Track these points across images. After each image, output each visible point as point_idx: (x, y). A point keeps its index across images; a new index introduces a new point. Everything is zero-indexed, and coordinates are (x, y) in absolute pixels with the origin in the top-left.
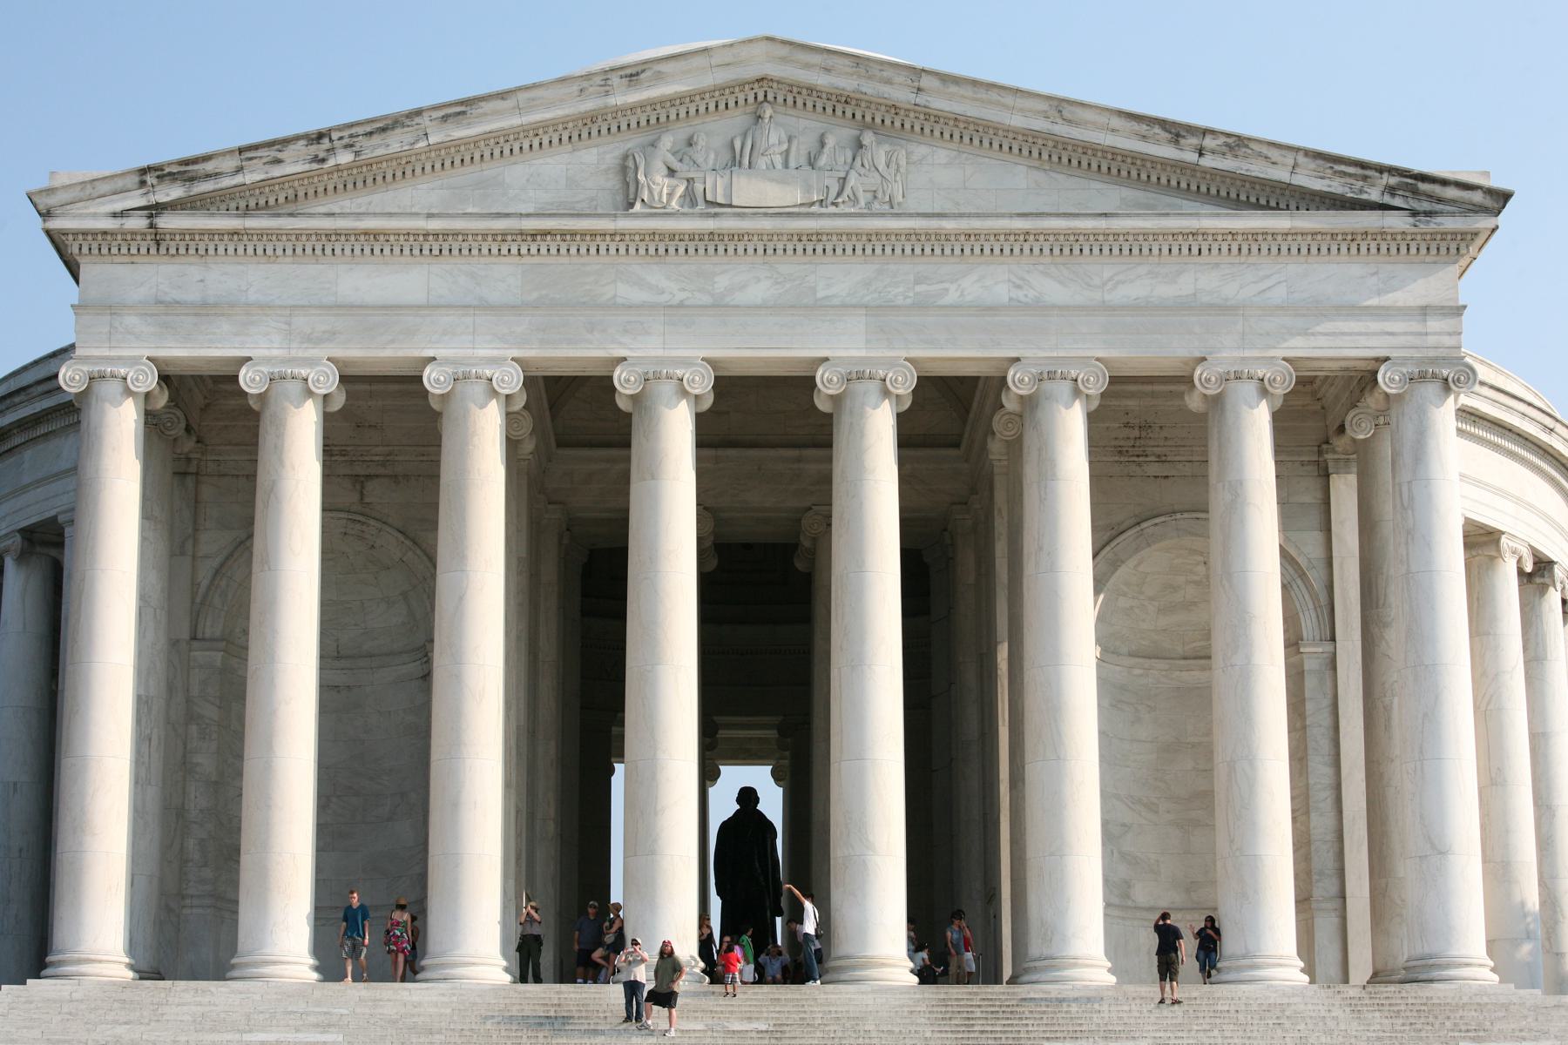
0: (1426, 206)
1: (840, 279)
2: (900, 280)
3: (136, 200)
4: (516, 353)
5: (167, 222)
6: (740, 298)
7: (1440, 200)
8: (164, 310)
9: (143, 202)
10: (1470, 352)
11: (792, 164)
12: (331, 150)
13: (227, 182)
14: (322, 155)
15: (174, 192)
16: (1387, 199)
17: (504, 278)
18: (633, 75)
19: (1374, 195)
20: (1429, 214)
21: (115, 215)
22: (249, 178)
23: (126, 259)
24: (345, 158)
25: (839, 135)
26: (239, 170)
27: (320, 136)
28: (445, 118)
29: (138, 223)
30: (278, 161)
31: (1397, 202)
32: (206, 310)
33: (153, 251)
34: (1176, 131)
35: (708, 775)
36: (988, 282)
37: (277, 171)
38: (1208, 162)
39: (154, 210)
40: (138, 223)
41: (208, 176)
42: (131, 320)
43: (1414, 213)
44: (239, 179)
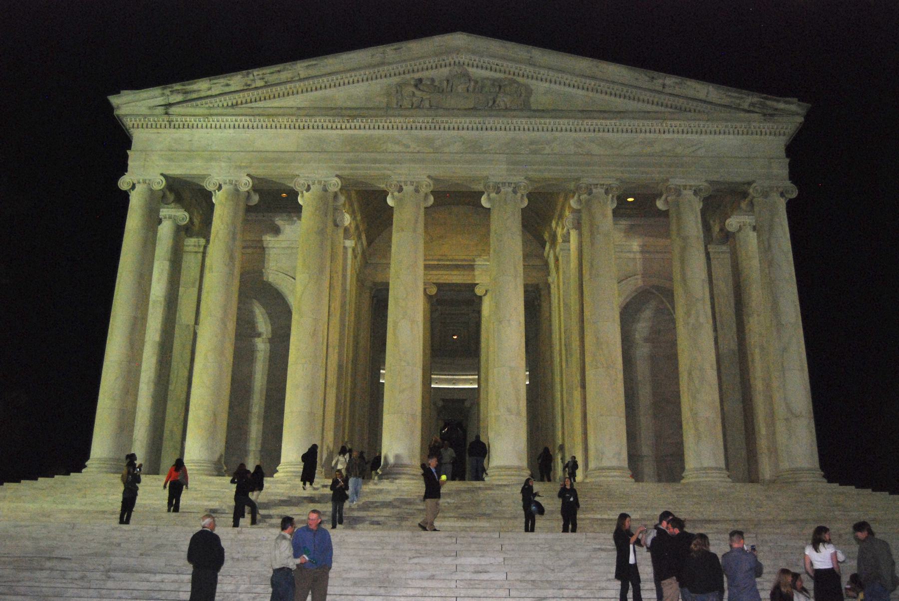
0: (770, 111)
3: (161, 101)
4: (338, 173)
5: (172, 110)
6: (447, 150)
7: (776, 109)
8: (172, 153)
9: (163, 103)
11: (471, 89)
12: (254, 80)
13: (203, 94)
14: (249, 83)
15: (180, 98)
16: (752, 108)
19: (746, 106)
20: (771, 115)
21: (150, 108)
22: (214, 92)
23: (155, 130)
24: (260, 83)
26: (210, 89)
28: (308, 67)
30: (228, 85)
31: (757, 110)
32: (191, 154)
33: (168, 126)
35: (427, 381)
37: (227, 89)
38: (667, 90)
39: (170, 105)
40: (161, 110)
41: (194, 91)
43: (765, 115)
44: (209, 93)
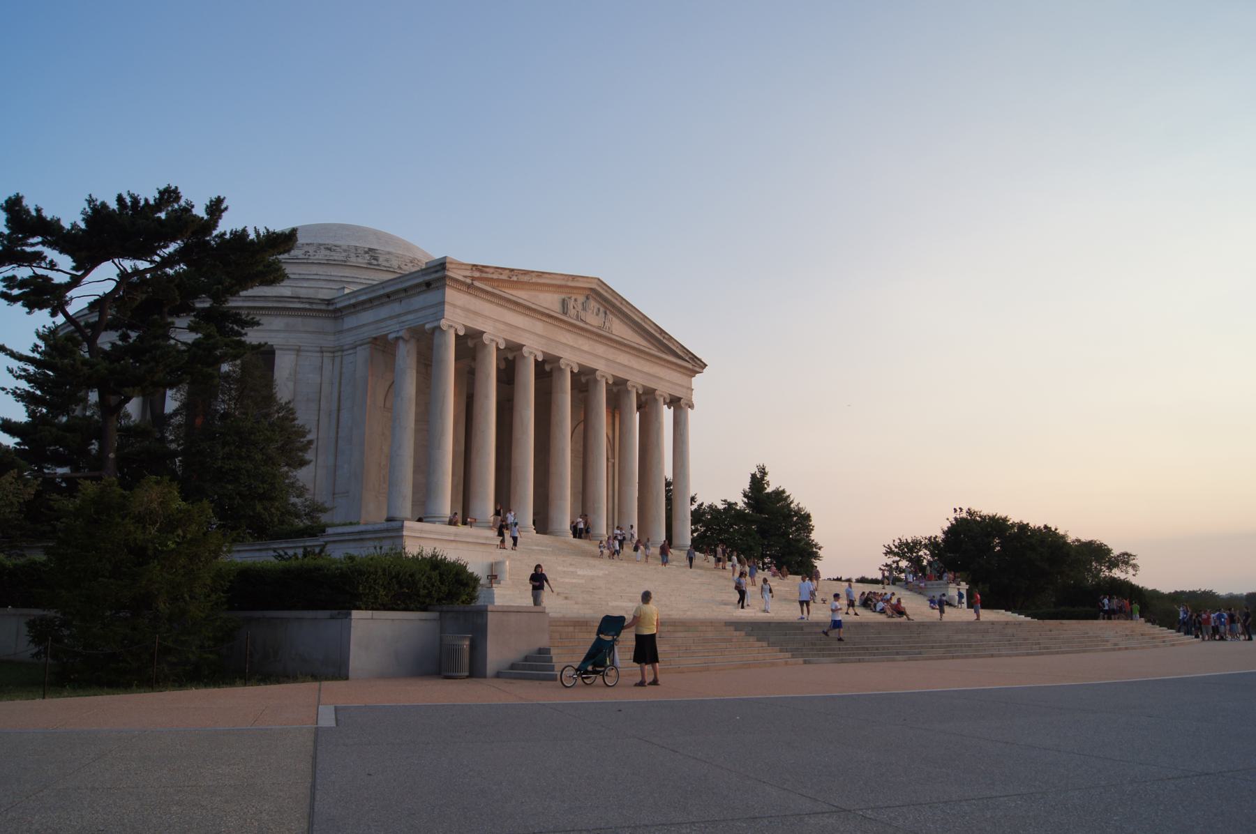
1: (600, 349)
2: (612, 354)
3: (468, 273)
10: (695, 400)
17: (538, 326)
18: (574, 277)
22: (495, 276)
24: (515, 278)
25: (602, 309)
27: (512, 270)
29: (469, 281)
32: (475, 313)
34: (662, 331)
36: (624, 358)
39: (473, 279)
42: (458, 311)
